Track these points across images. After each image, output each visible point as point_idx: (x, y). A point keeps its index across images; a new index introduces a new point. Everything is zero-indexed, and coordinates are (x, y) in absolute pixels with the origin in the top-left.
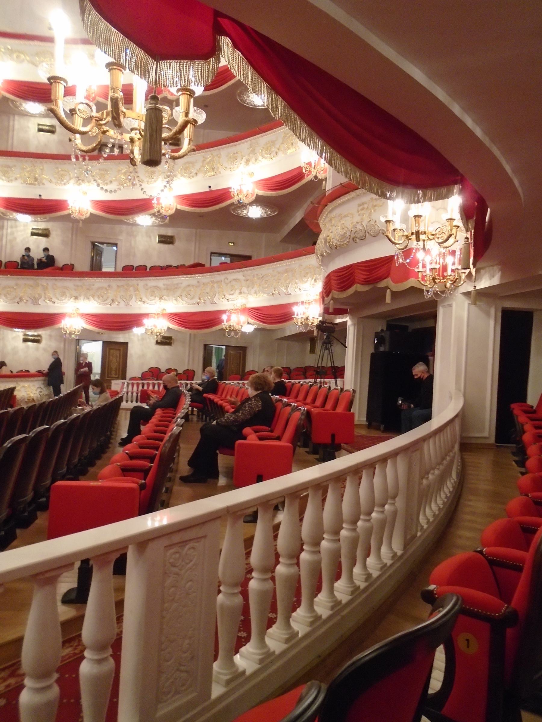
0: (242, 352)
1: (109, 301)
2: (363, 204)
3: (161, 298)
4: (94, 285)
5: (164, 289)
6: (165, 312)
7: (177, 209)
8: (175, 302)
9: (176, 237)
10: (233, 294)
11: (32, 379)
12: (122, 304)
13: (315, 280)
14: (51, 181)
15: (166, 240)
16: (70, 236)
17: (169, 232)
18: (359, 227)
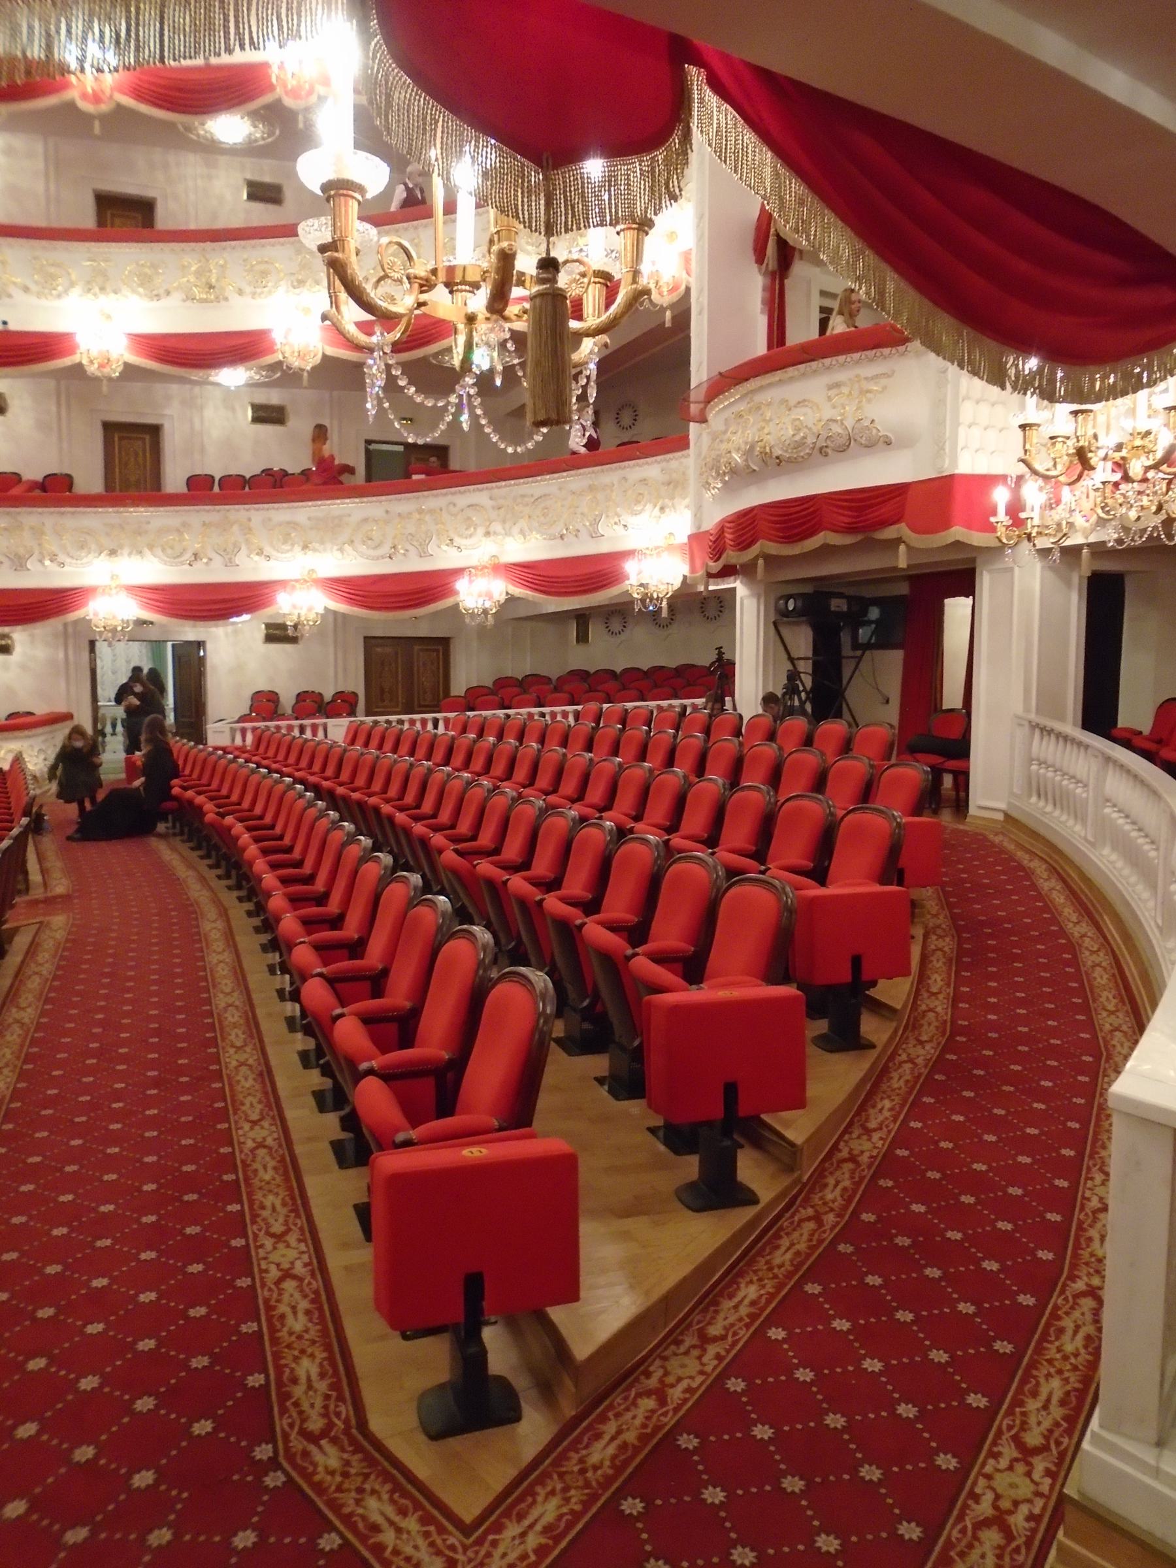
0: (440, 648)
1: (188, 556)
2: (837, 385)
3: (305, 547)
4: (148, 523)
5: (311, 528)
6: (314, 576)
7: (325, 356)
8: (338, 554)
9: (289, 409)
10: (471, 536)
11: (26, 733)
12: (218, 561)
13: (662, 509)
14: (26, 289)
15: (268, 415)
16: (54, 409)
17: (274, 397)
18: (836, 429)
